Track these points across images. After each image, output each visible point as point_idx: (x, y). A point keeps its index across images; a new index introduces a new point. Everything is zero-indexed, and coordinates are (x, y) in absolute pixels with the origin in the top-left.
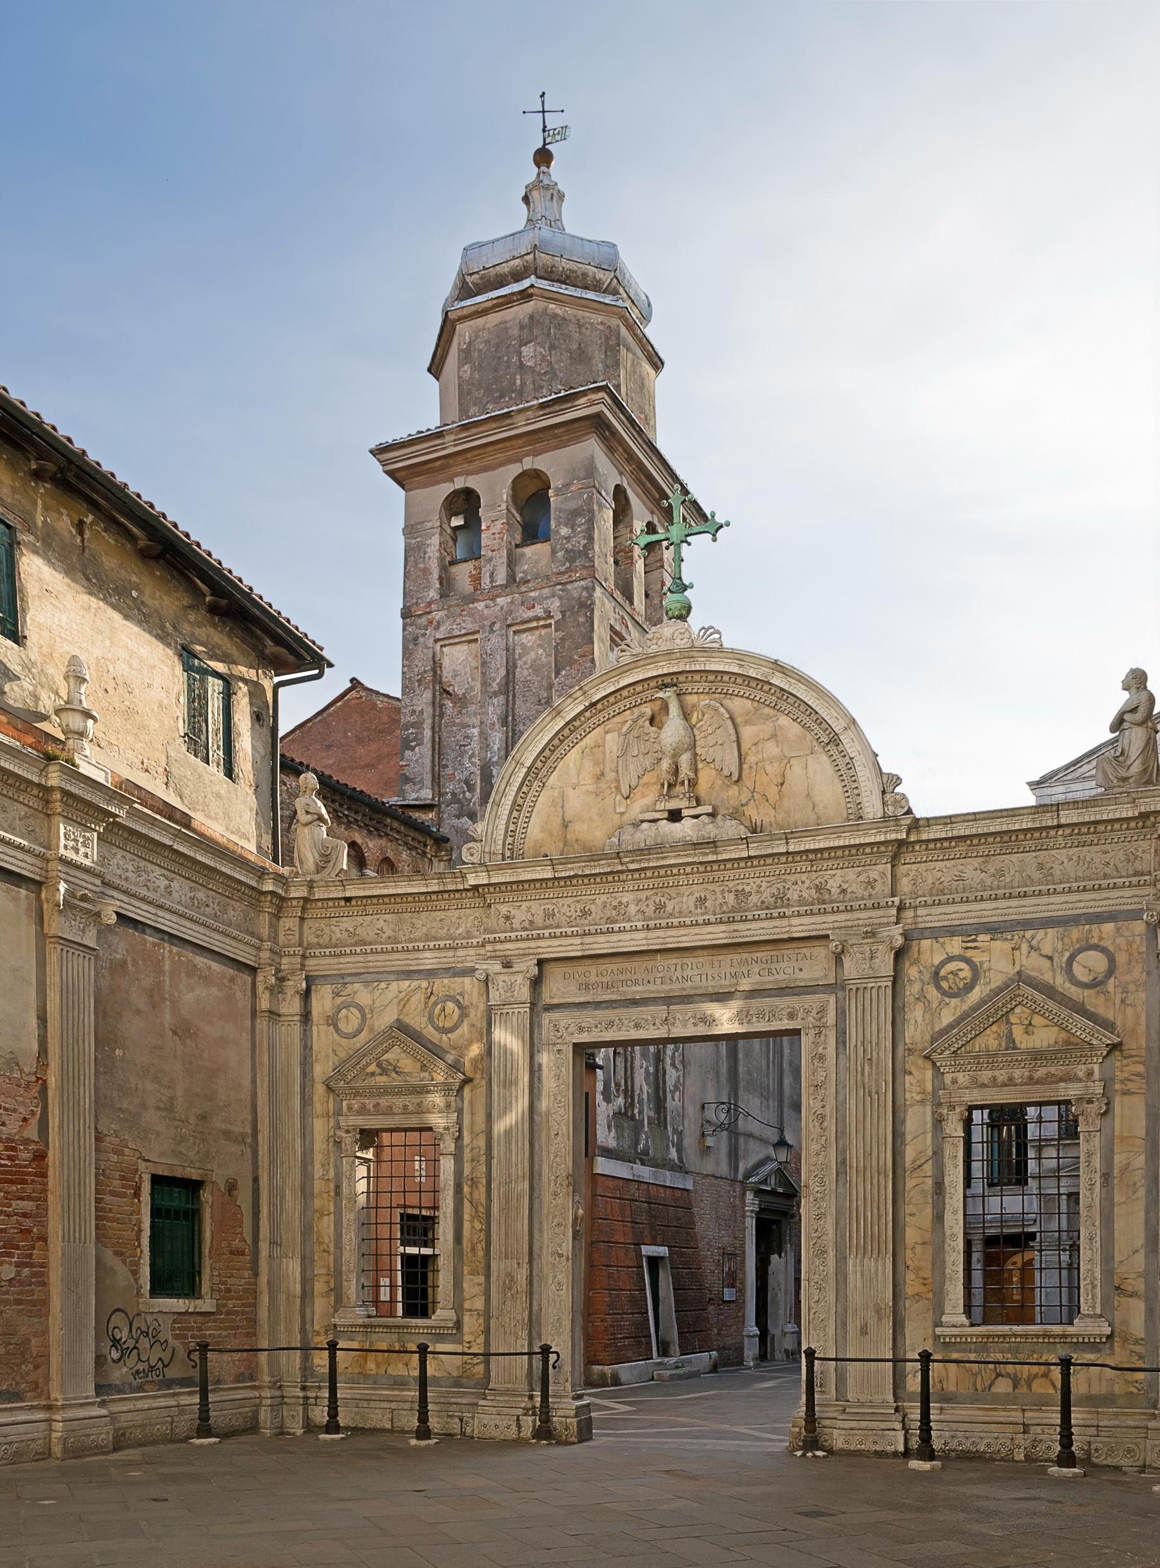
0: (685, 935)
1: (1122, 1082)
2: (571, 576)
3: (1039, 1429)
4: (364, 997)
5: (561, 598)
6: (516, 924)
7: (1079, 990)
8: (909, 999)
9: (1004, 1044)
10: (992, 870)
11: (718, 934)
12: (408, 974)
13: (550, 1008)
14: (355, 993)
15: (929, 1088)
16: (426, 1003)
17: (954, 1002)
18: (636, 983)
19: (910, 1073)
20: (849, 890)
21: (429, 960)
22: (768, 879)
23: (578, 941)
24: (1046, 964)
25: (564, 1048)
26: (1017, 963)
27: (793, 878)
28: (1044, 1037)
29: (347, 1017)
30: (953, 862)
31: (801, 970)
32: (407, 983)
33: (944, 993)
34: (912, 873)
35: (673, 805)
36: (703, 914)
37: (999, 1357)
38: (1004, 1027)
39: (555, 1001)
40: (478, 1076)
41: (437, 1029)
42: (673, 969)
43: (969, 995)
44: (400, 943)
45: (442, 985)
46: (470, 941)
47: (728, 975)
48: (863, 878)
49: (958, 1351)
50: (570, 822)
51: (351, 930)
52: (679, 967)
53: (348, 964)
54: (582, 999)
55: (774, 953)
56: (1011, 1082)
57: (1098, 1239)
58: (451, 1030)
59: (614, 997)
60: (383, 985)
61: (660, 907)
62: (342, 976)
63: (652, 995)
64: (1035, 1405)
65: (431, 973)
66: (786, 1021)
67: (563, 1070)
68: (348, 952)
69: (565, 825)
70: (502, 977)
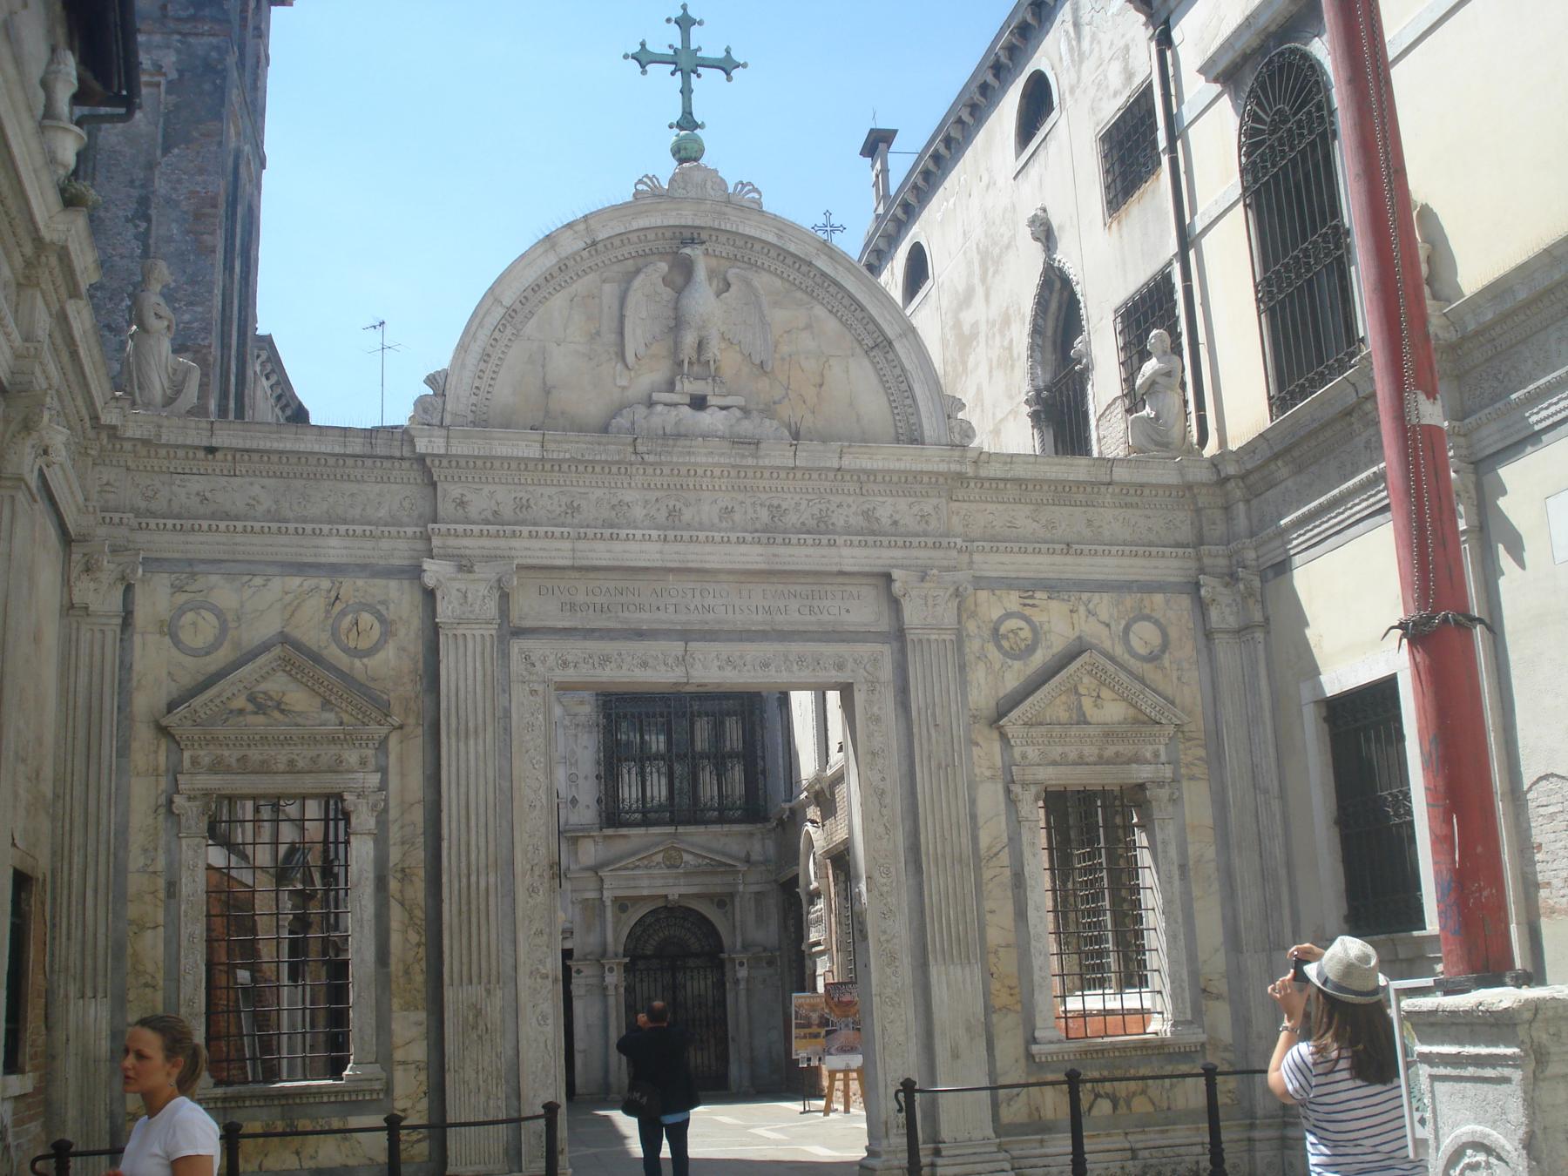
0: (709, 554)
1: (1187, 766)
2: (195, 27)
3: (1146, 1153)
4: (225, 595)
5: (178, 51)
6: (473, 511)
7: (1139, 664)
8: (970, 658)
9: (1074, 716)
10: (1043, 521)
11: (752, 556)
12: (300, 568)
13: (519, 632)
14: (211, 589)
15: (999, 763)
16: (327, 612)
17: (1017, 665)
18: (641, 609)
19: (977, 744)
20: (902, 522)
21: (334, 549)
22: (809, 497)
23: (567, 545)
24: (1104, 632)
25: (540, 688)
26: (1076, 626)
27: (836, 499)
28: (1113, 711)
29: (194, 624)
30: (1005, 506)
31: (848, 611)
32: (297, 581)
33: (1006, 654)
34: (964, 512)
35: (698, 387)
36: (726, 530)
37: (1096, 1074)
38: (1073, 698)
39: (527, 624)
40: (411, 721)
41: (346, 650)
42: (690, 595)
43: (1032, 658)
44: (287, 521)
45: (353, 588)
46: (402, 530)
47: (760, 610)
48: (915, 509)
49: (1053, 1071)
50: (554, 387)
51: (208, 494)
52: (697, 593)
53: (201, 544)
54: (567, 624)
55: (815, 587)
56: (1081, 761)
57: (1182, 937)
58: (371, 652)
59: (612, 625)
60: (258, 581)
61: (673, 513)
62: (190, 562)
63: (664, 626)
64: (1137, 1126)
65: (335, 570)
66: (834, 673)
67: (541, 717)
68: (205, 527)
69: (547, 391)
70: (457, 585)
